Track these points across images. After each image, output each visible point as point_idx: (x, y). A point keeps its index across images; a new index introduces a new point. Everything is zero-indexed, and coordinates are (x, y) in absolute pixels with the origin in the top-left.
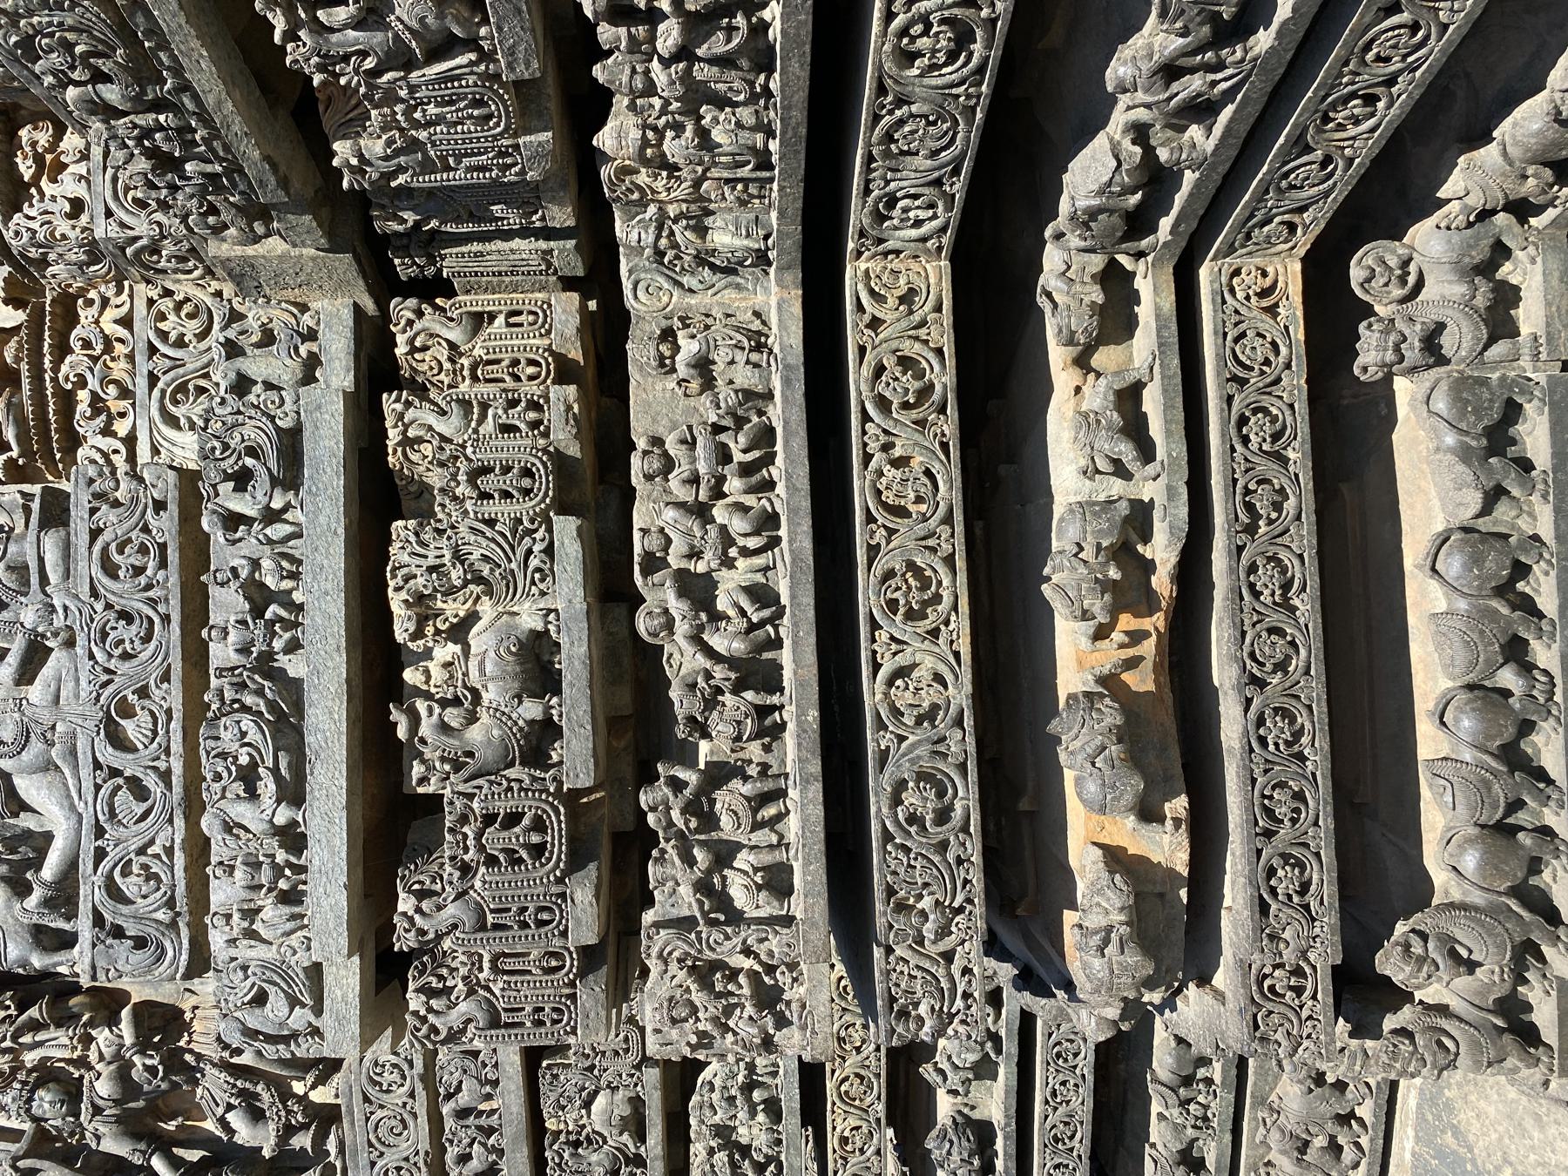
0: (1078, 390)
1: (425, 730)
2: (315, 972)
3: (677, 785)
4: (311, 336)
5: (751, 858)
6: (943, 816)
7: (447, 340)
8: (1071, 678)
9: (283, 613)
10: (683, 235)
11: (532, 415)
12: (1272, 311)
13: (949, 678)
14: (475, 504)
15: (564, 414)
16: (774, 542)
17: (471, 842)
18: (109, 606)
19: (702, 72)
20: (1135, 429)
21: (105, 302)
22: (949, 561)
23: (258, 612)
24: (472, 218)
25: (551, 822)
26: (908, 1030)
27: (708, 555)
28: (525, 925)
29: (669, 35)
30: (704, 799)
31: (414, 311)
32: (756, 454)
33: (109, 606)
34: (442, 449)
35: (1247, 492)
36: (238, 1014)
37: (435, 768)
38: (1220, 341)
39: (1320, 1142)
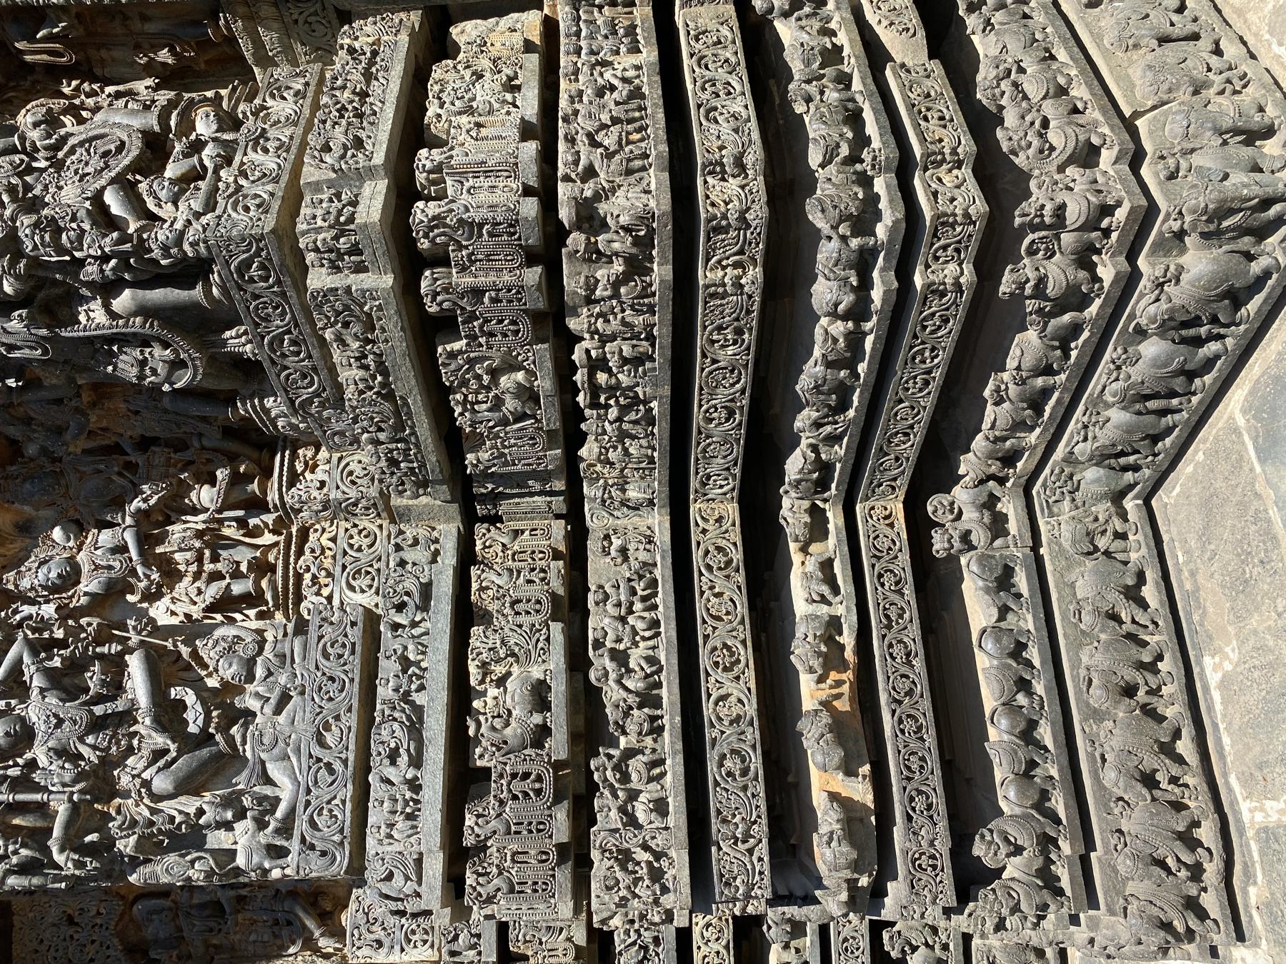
0: (803, 563)
1: (483, 730)
2: (419, 862)
3: (610, 757)
4: (436, 541)
6: (745, 772)
8: (808, 704)
9: (417, 671)
10: (615, 493)
11: (542, 575)
12: (891, 525)
13: (745, 701)
16: (658, 634)
18: (324, 674)
19: (625, 426)
20: (831, 581)
21: (324, 530)
22: (744, 642)
23: (405, 671)
24: (519, 486)
27: (626, 640)
29: (613, 413)
32: (649, 591)
33: (324, 674)
35: (885, 609)
36: (378, 885)
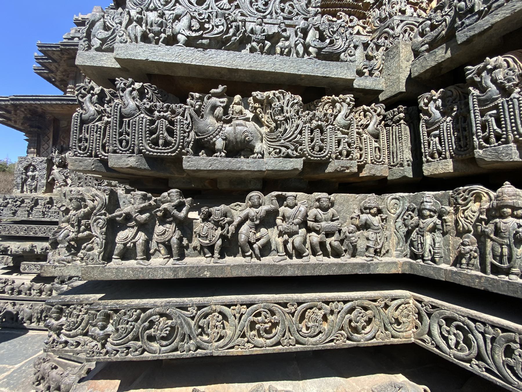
1: (214, 100)
3: (179, 207)
4: (371, 74)
5: (141, 241)
7: (369, 124)
11: (345, 153)
14: (309, 127)
15: (345, 166)
17: (162, 114)
21: (364, 28)
23: (268, 37)
25: (168, 149)
26: (52, 313)
27: (285, 225)
28: (121, 134)
30: (171, 219)
31: (380, 112)
34: (332, 115)
37: (197, 102)
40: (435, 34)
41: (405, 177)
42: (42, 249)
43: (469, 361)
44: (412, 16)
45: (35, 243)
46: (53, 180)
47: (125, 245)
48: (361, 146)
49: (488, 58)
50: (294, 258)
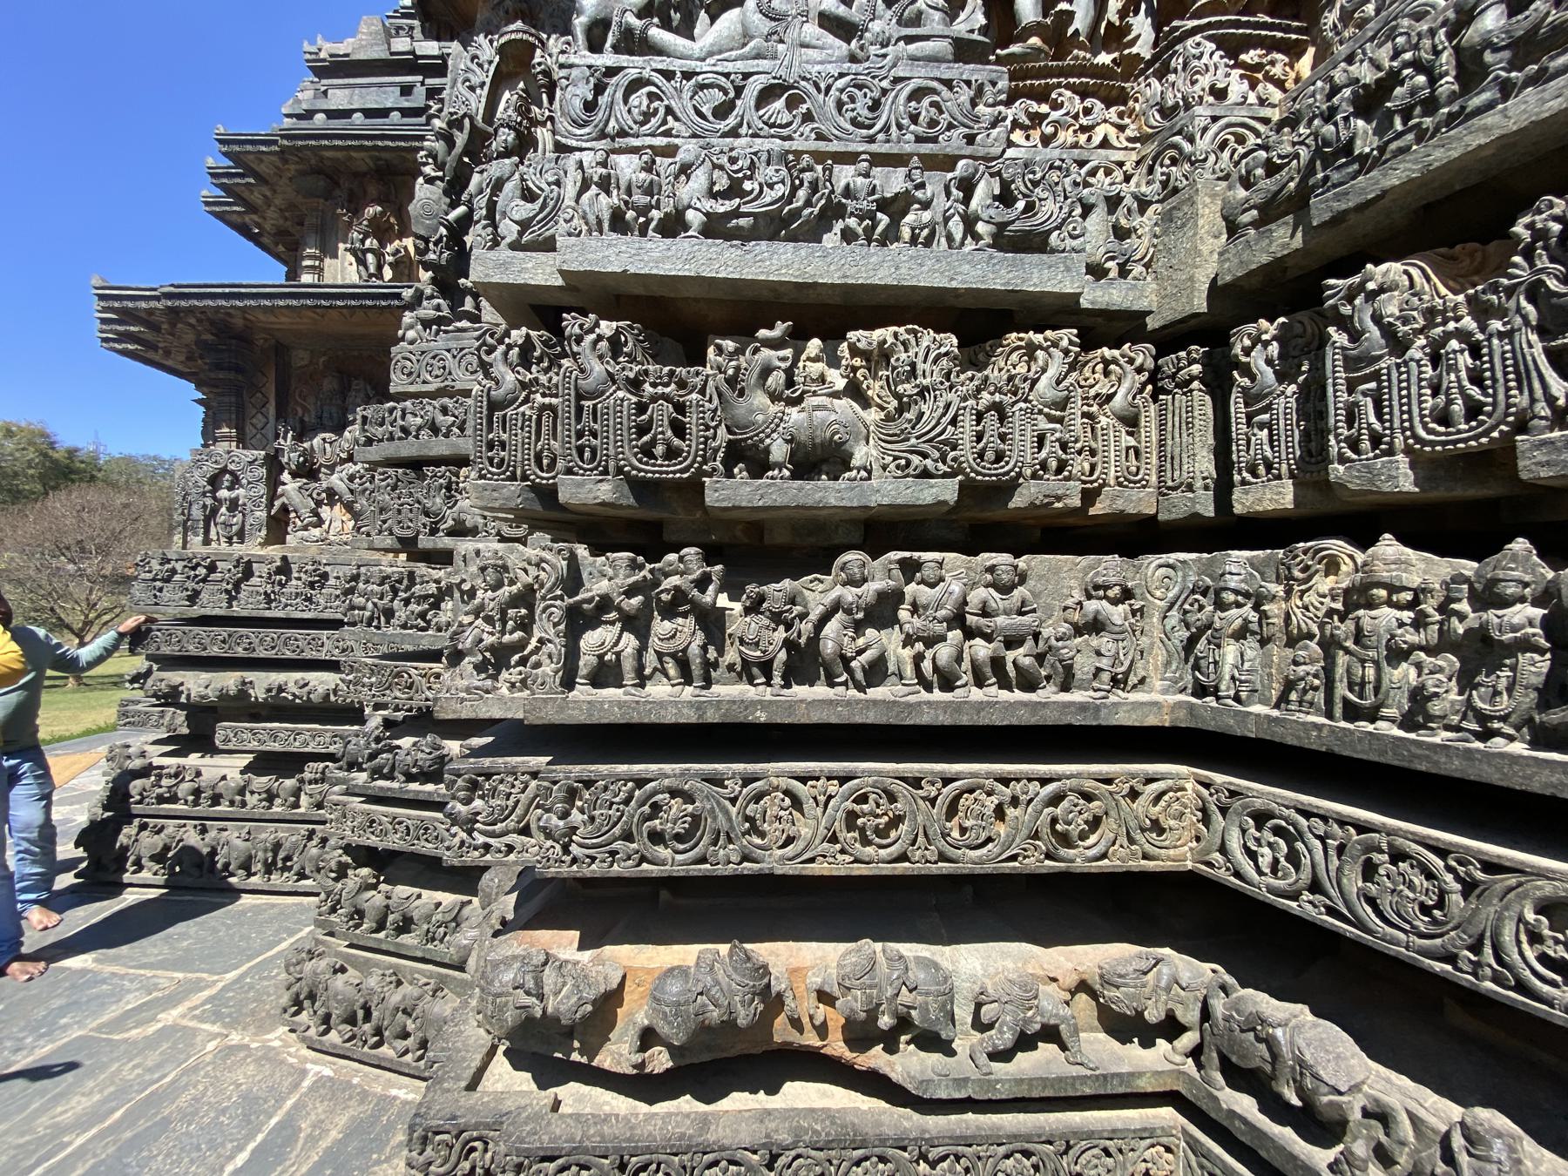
0: (1054, 980)
1: (766, 353)
2: (549, 245)
3: (703, 583)
4: (1123, 272)
5: (629, 650)
6: (656, 837)
9: (880, 229)
11: (1053, 464)
13: (790, 850)
17: (660, 389)
18: (884, 92)
21: (1121, 128)
22: (903, 857)
23: (884, 205)
26: (459, 790)
27: (917, 622)
28: (580, 435)
30: (687, 607)
32: (1012, 673)
33: (884, 92)
36: (517, 176)
38: (1106, 1135)
39: (411, 1026)
40: (1274, 188)
41: (1196, 515)
42: (269, 690)
43: (1295, 896)
44: (1242, 103)
45: (250, 676)
46: (285, 509)
47: (601, 657)
48: (1094, 445)
49: (1369, 266)
50: (936, 691)
